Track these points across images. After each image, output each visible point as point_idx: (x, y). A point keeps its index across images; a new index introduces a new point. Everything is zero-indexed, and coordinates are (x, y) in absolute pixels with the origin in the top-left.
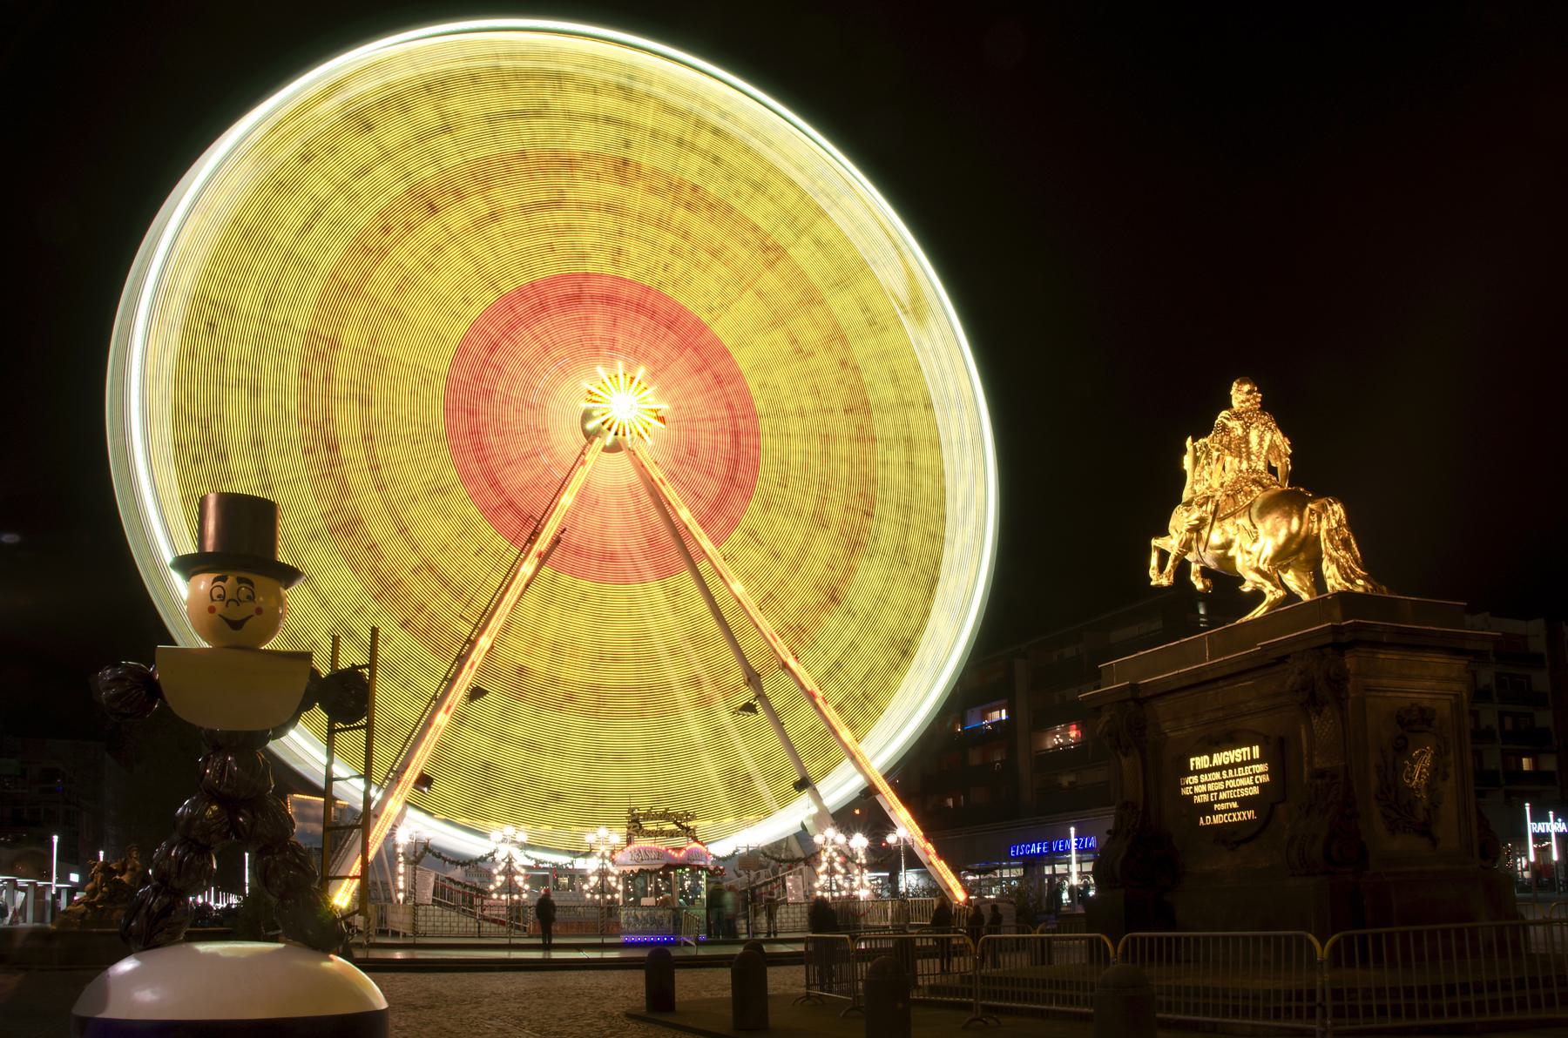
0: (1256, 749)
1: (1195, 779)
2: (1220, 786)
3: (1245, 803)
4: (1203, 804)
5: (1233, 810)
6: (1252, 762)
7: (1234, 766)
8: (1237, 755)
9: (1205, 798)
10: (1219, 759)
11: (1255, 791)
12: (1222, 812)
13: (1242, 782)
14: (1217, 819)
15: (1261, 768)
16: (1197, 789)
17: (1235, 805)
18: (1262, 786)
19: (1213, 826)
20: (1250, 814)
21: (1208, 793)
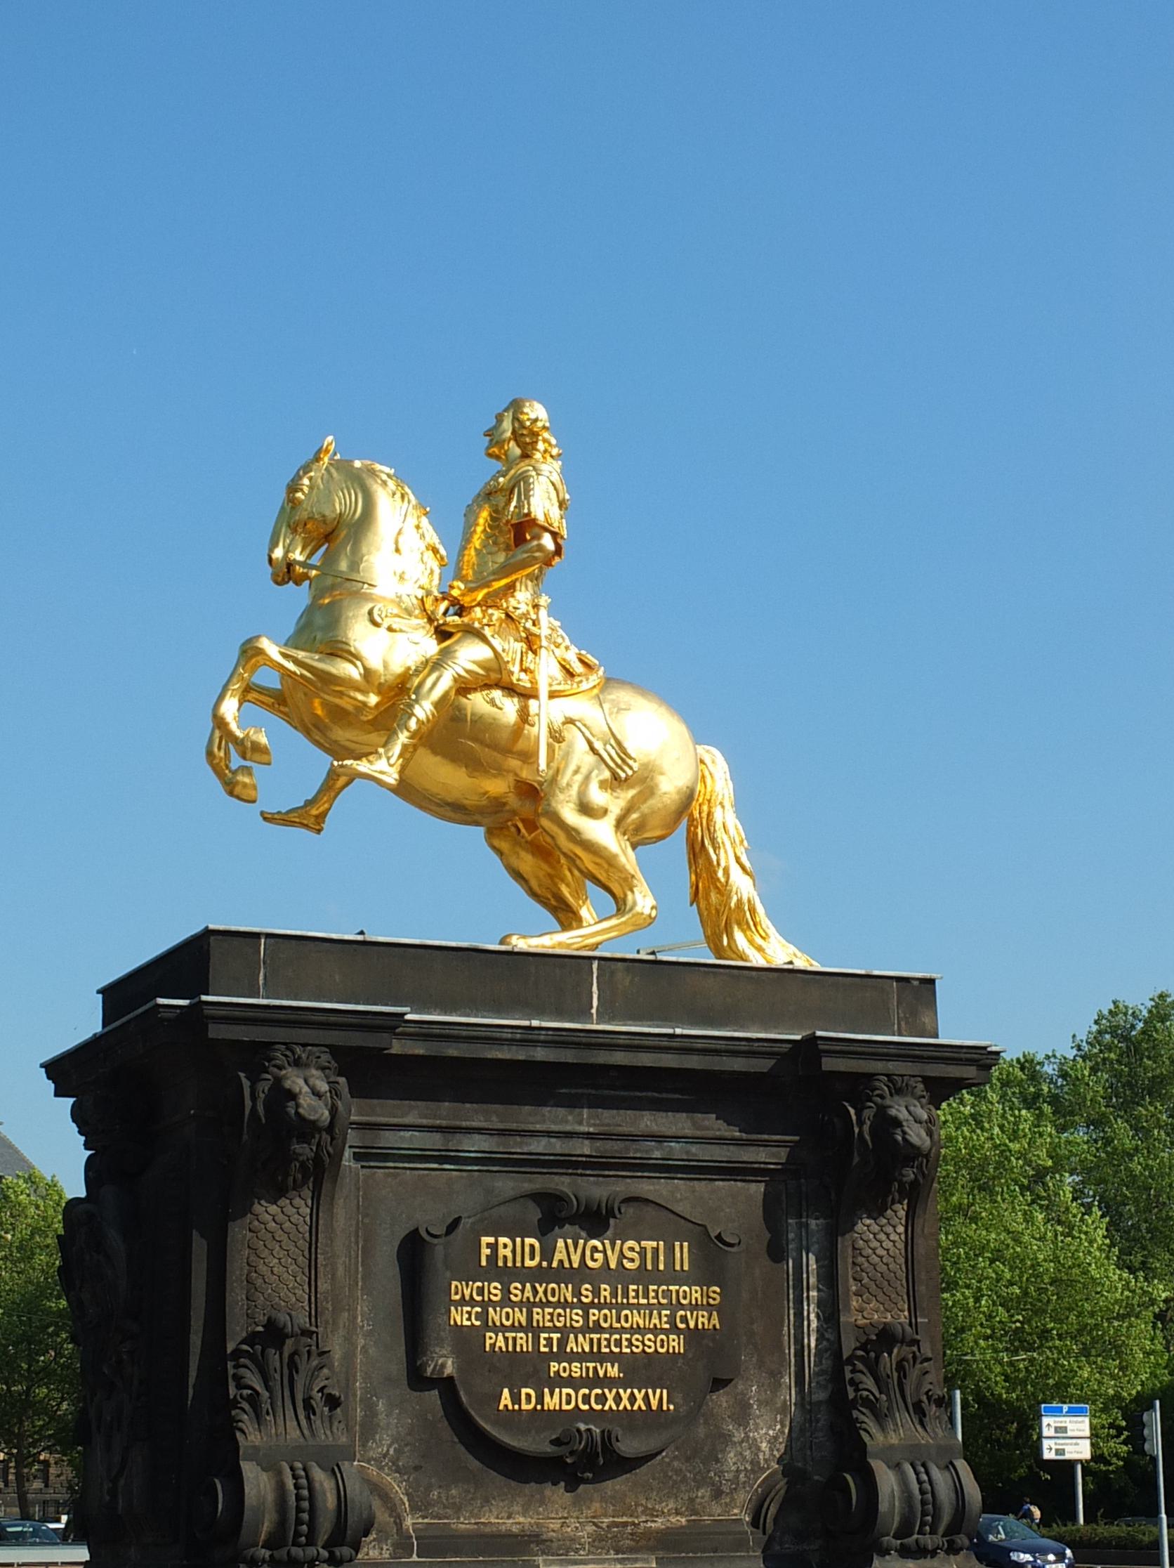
0: (683, 1254)
3: (641, 1370)
4: (514, 1357)
5: (608, 1382)
6: (672, 1276)
7: (619, 1277)
8: (629, 1252)
9: (523, 1341)
10: (566, 1251)
11: (676, 1344)
13: (637, 1319)
14: (551, 1402)
15: (696, 1293)
17: (613, 1371)
18: (693, 1336)
19: (542, 1417)
20: (658, 1397)
21: (532, 1329)
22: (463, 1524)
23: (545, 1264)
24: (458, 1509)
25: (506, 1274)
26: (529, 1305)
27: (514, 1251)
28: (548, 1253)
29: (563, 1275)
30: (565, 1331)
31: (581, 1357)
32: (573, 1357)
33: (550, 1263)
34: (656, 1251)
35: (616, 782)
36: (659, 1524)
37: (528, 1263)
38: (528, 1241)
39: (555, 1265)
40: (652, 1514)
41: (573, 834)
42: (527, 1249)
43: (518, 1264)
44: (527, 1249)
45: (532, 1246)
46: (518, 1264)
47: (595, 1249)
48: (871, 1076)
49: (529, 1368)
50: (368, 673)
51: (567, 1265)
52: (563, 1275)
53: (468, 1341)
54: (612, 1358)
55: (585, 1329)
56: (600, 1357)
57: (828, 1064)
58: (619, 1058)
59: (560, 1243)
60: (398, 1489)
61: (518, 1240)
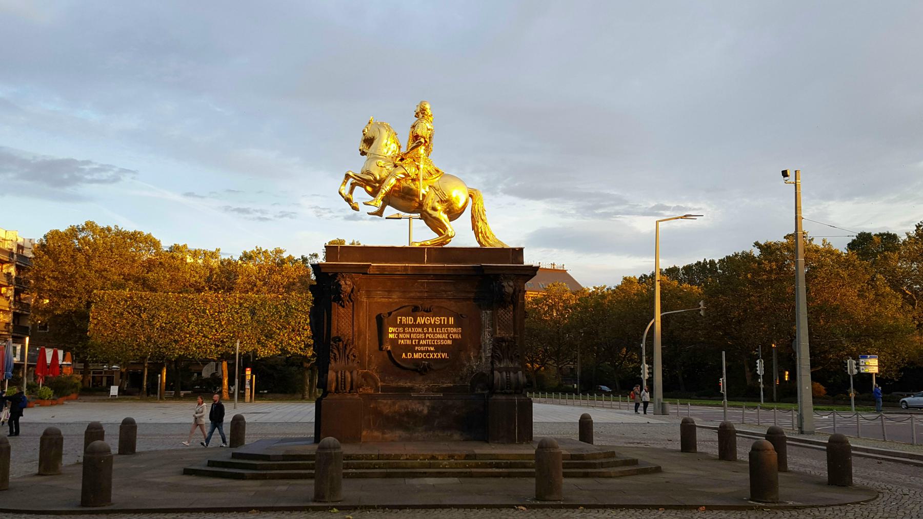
0: (451, 320)
1: (401, 329)
2: (422, 336)
3: (439, 348)
5: (431, 351)
6: (449, 326)
7: (434, 326)
9: (409, 342)
10: (421, 320)
11: (449, 342)
12: (422, 352)
14: (416, 356)
15: (454, 330)
16: (401, 336)
17: (432, 349)
18: (454, 340)
19: (413, 359)
21: (412, 339)
22: (394, 384)
24: (392, 381)
25: (404, 326)
26: (410, 333)
28: (415, 321)
29: (419, 326)
30: (420, 340)
31: (424, 345)
32: (422, 345)
35: (442, 201)
36: (445, 385)
40: (443, 383)
41: (430, 215)
48: (499, 275)
49: (410, 349)
50: (375, 178)
52: (419, 326)
53: (394, 342)
54: (432, 346)
55: (425, 339)
56: (429, 346)
57: (486, 272)
58: (430, 272)
60: (377, 377)
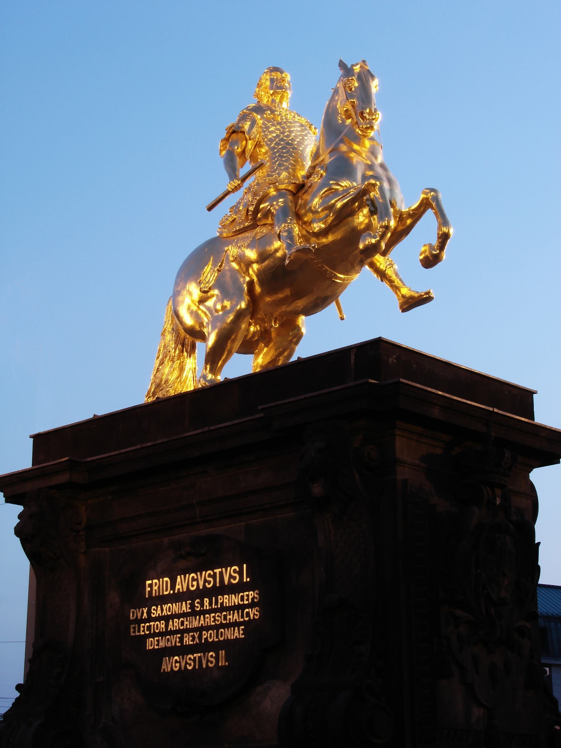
10: (183, 583)
23: (172, 592)
27: (159, 588)
33: (174, 590)
34: (221, 573)
37: (165, 593)
38: (166, 579)
39: (176, 592)
42: (165, 583)
43: (161, 594)
44: (165, 583)
45: (167, 581)
46: (161, 594)
47: (193, 579)
51: (181, 591)
59: (179, 577)
61: (161, 580)
